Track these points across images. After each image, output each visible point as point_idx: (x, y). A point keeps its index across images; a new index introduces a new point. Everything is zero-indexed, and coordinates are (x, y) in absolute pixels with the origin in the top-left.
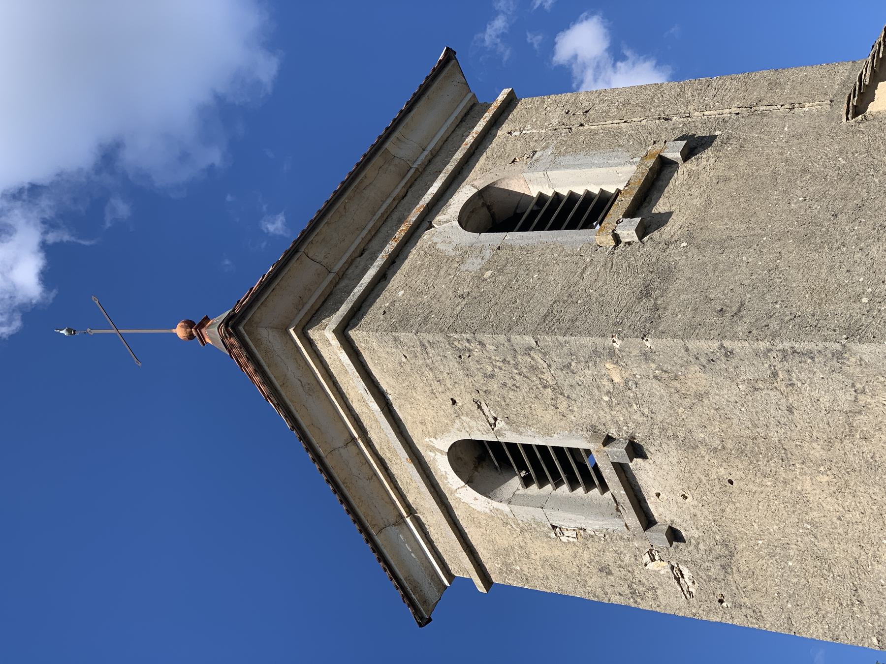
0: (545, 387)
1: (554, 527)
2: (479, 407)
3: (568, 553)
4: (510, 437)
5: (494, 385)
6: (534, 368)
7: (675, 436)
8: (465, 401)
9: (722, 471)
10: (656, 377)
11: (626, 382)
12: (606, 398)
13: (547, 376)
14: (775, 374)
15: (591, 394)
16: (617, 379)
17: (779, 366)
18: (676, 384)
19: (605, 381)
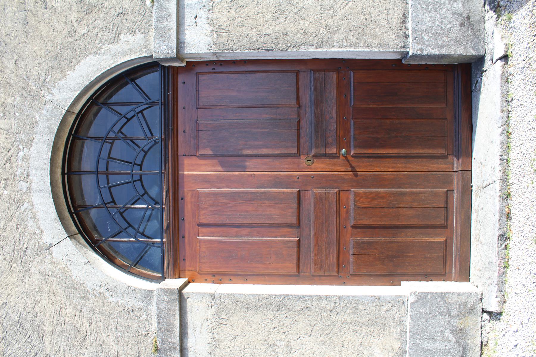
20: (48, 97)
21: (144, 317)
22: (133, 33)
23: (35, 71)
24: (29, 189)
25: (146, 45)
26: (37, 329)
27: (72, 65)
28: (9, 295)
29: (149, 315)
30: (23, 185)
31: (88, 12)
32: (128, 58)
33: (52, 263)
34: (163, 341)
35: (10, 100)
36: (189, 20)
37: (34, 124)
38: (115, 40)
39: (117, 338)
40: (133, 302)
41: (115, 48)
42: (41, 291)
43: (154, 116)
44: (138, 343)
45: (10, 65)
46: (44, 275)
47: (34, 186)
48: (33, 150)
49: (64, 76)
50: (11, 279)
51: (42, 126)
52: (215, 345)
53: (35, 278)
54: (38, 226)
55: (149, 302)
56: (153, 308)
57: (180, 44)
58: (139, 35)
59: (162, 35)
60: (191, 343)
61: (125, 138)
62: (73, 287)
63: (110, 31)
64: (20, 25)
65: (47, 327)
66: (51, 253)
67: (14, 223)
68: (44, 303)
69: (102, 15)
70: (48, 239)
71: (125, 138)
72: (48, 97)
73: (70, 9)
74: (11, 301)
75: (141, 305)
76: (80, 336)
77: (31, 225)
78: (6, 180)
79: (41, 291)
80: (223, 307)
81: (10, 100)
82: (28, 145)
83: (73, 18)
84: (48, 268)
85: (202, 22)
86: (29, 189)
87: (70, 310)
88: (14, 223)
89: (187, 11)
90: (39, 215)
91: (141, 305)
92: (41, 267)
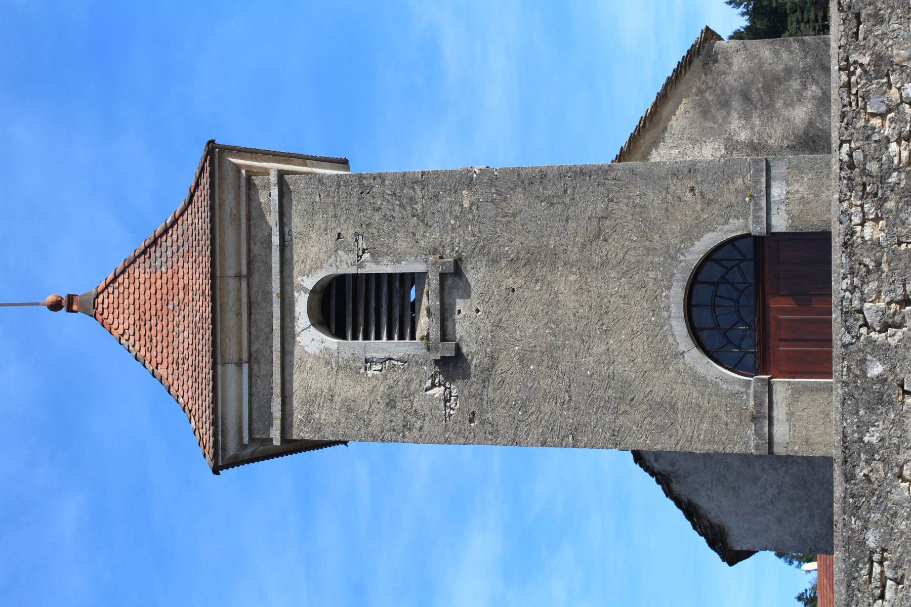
0: (413, 216)
1: (367, 361)
2: (357, 240)
3: (367, 387)
4: (371, 268)
5: (377, 217)
6: (412, 200)
7: (489, 253)
8: (349, 236)
9: (511, 280)
10: (492, 201)
11: (472, 205)
12: (453, 222)
13: (418, 207)
14: (565, 191)
15: (444, 219)
16: (466, 205)
17: (569, 183)
18: (504, 205)
19: (457, 208)
20: (682, 258)
21: (745, 397)
22: (738, 218)
23: (674, 241)
24: (670, 317)
25: (746, 226)
26: (673, 407)
27: (698, 238)
28: (655, 385)
29: (748, 396)
30: (665, 314)
31: (708, 204)
32: (735, 234)
33: (684, 364)
34: (758, 412)
35: (657, 259)
36: (774, 211)
37: (673, 275)
38: (726, 222)
39: (727, 412)
40: (737, 387)
41: (726, 227)
42: (676, 382)
43: (748, 267)
44: (740, 414)
45: (657, 237)
46: (678, 371)
47: (672, 315)
48: (672, 292)
49: (693, 245)
50: (656, 375)
51: (678, 276)
52: (791, 415)
53: (672, 374)
54: (675, 340)
55: (749, 388)
56: (751, 390)
57: (769, 225)
58: (741, 220)
59: (757, 220)
60: (775, 414)
61: (728, 282)
62: (697, 379)
63: (722, 216)
64: (663, 212)
65: (680, 406)
66: (684, 357)
67: (659, 338)
68: (678, 390)
69: (717, 206)
70: (681, 348)
71: (728, 282)
72: (682, 258)
73: (696, 202)
74: (656, 389)
75: (743, 390)
76: (702, 411)
77: (671, 340)
78: (653, 311)
79: (676, 382)
80: (797, 392)
81: (657, 259)
82: (669, 288)
83: (698, 208)
84: (681, 366)
85: (783, 213)
86: (670, 317)
87: (695, 394)
88: (659, 338)
89: (773, 205)
90: (676, 333)
91: (743, 390)
92: (677, 367)
